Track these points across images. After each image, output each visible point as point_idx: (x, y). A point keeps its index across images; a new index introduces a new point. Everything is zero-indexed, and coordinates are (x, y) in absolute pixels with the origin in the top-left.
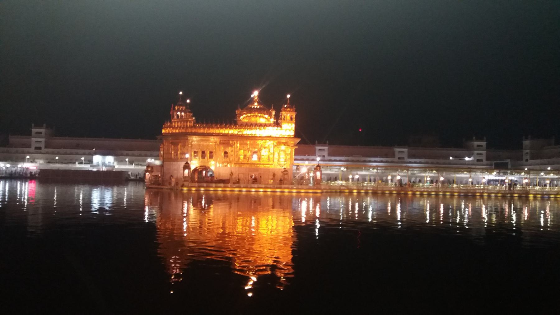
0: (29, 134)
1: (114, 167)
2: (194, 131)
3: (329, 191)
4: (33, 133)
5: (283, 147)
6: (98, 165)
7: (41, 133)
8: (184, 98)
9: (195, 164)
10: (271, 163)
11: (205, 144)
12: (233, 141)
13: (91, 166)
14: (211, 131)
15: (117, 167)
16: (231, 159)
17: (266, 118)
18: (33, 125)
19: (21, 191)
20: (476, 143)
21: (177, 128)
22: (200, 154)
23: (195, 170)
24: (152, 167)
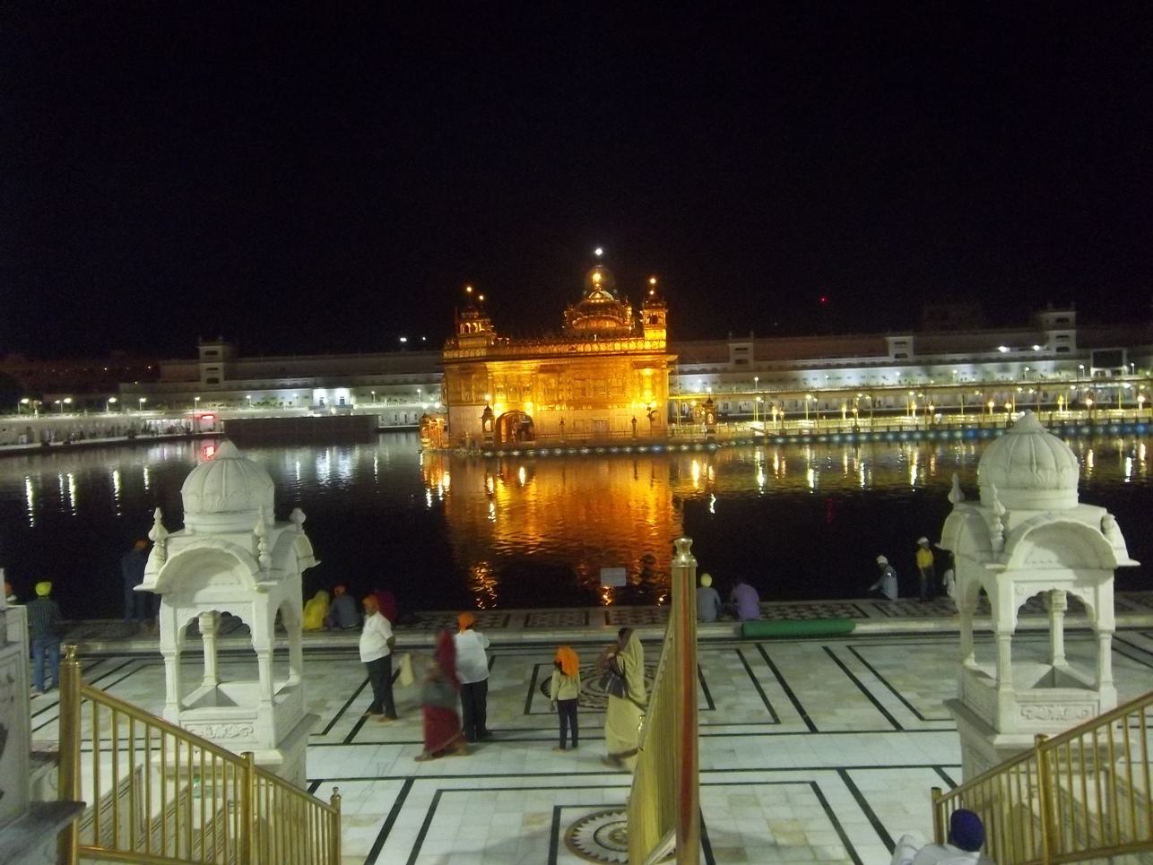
0: (193, 355)
2: (496, 352)
4: (202, 355)
5: (647, 372)
7: (215, 353)
9: (500, 407)
11: (516, 373)
13: (311, 408)
16: (560, 397)
17: (616, 321)
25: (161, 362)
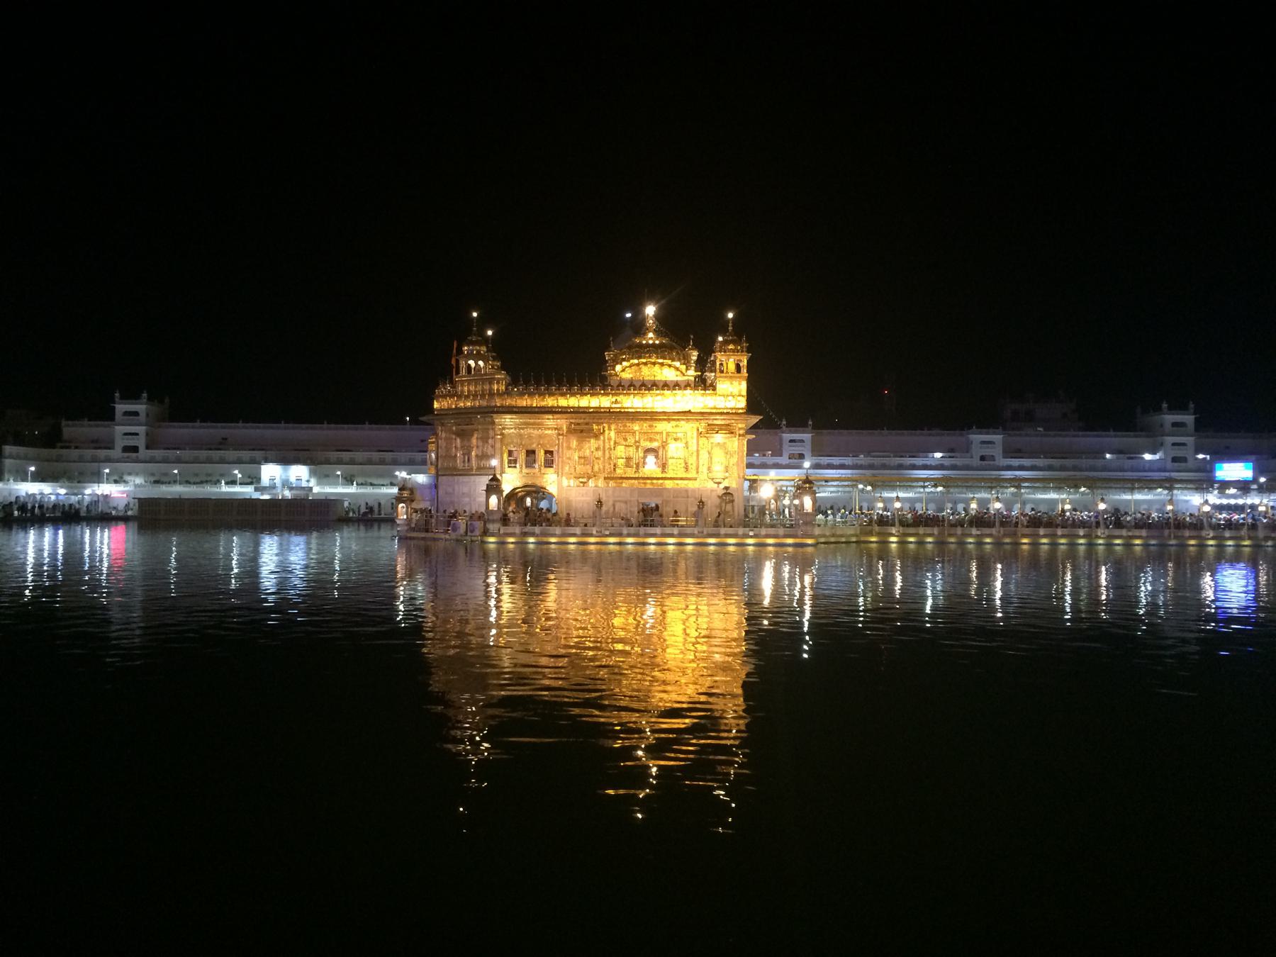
0: (108, 415)
1: (311, 489)
2: (509, 402)
3: (833, 540)
5: (719, 438)
6: (273, 487)
7: (136, 414)
8: (483, 323)
9: (511, 480)
10: (692, 474)
12: (598, 424)
13: (256, 489)
14: (550, 402)
15: (316, 490)
16: (596, 468)
17: (677, 369)
18: (117, 395)
19: (93, 551)
20: (1169, 418)
21: (467, 397)
22: (522, 457)
23: (512, 494)
24: (412, 491)
25: (64, 423)
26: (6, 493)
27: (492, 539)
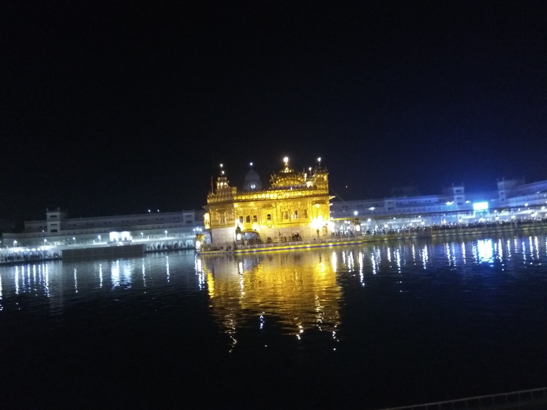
0: (44, 218)
2: (239, 198)
6: (115, 241)
7: (56, 216)
18: (47, 209)
19: (37, 274)
20: (455, 189)
21: (221, 197)
25: (25, 222)
26: (6, 253)
27: (239, 251)
